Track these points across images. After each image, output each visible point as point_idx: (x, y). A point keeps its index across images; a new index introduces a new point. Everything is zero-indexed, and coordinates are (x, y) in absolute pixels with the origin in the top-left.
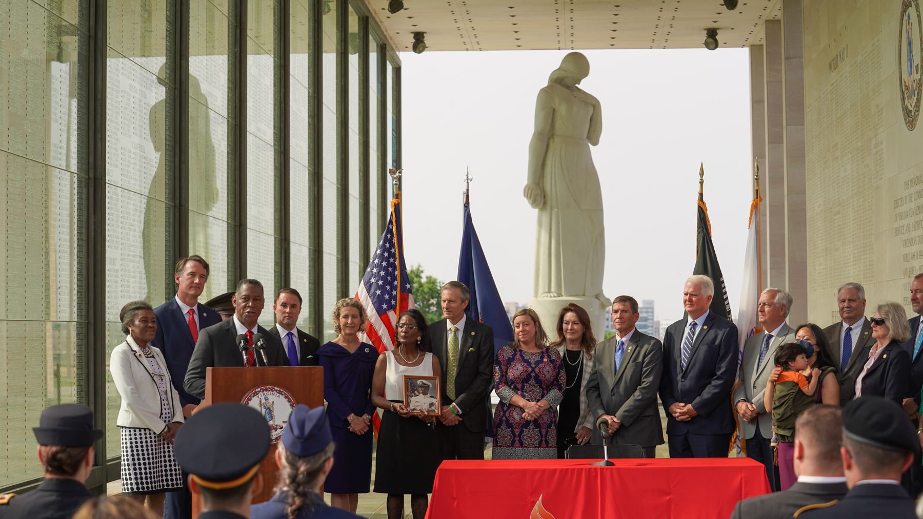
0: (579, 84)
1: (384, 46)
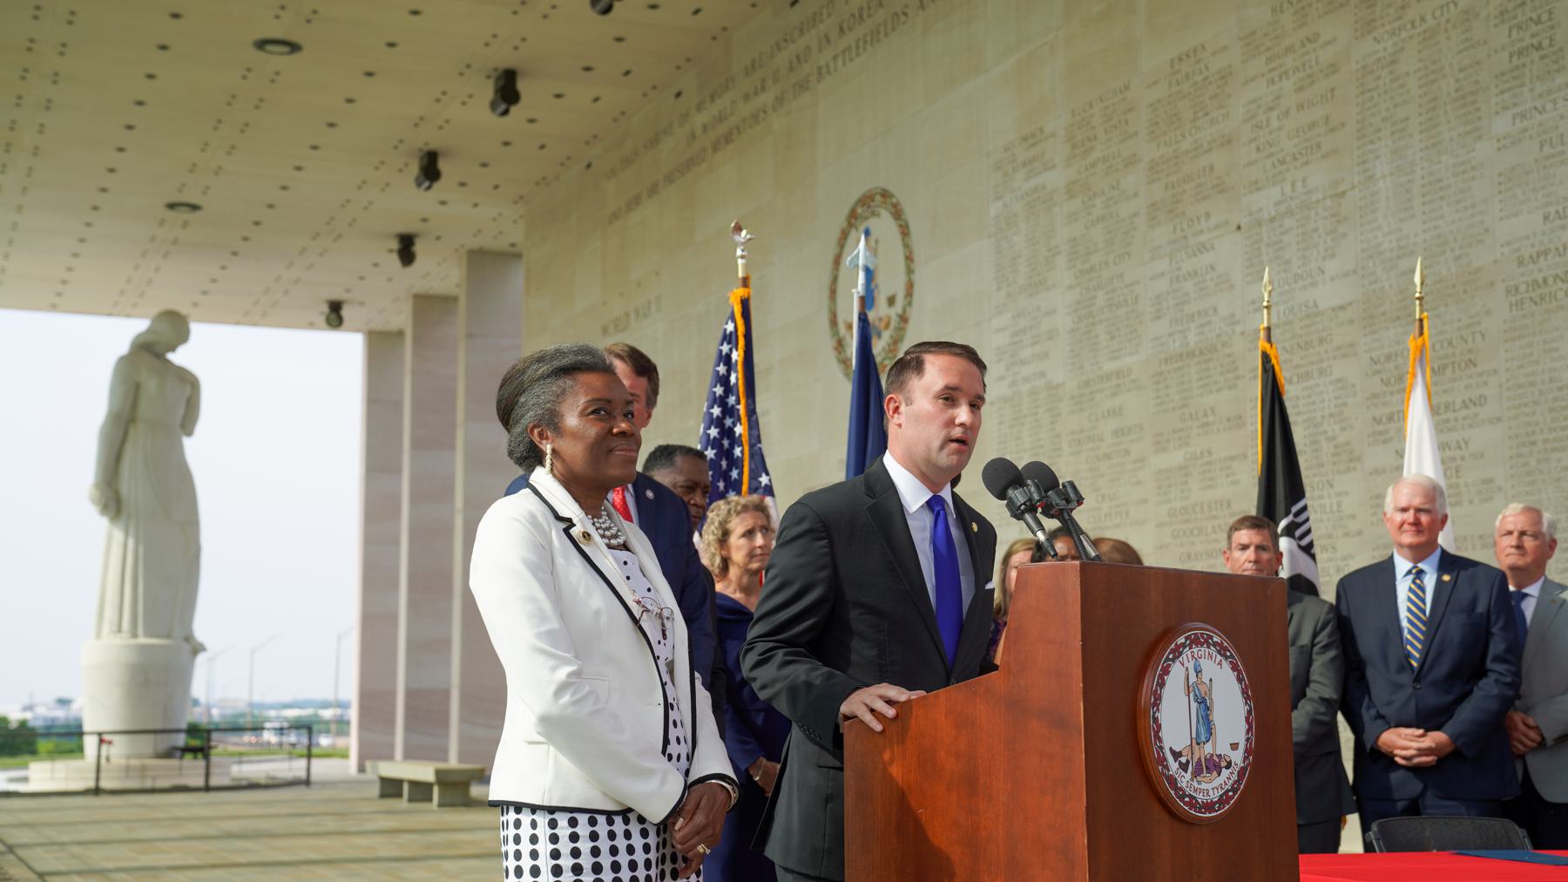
0: (173, 349)
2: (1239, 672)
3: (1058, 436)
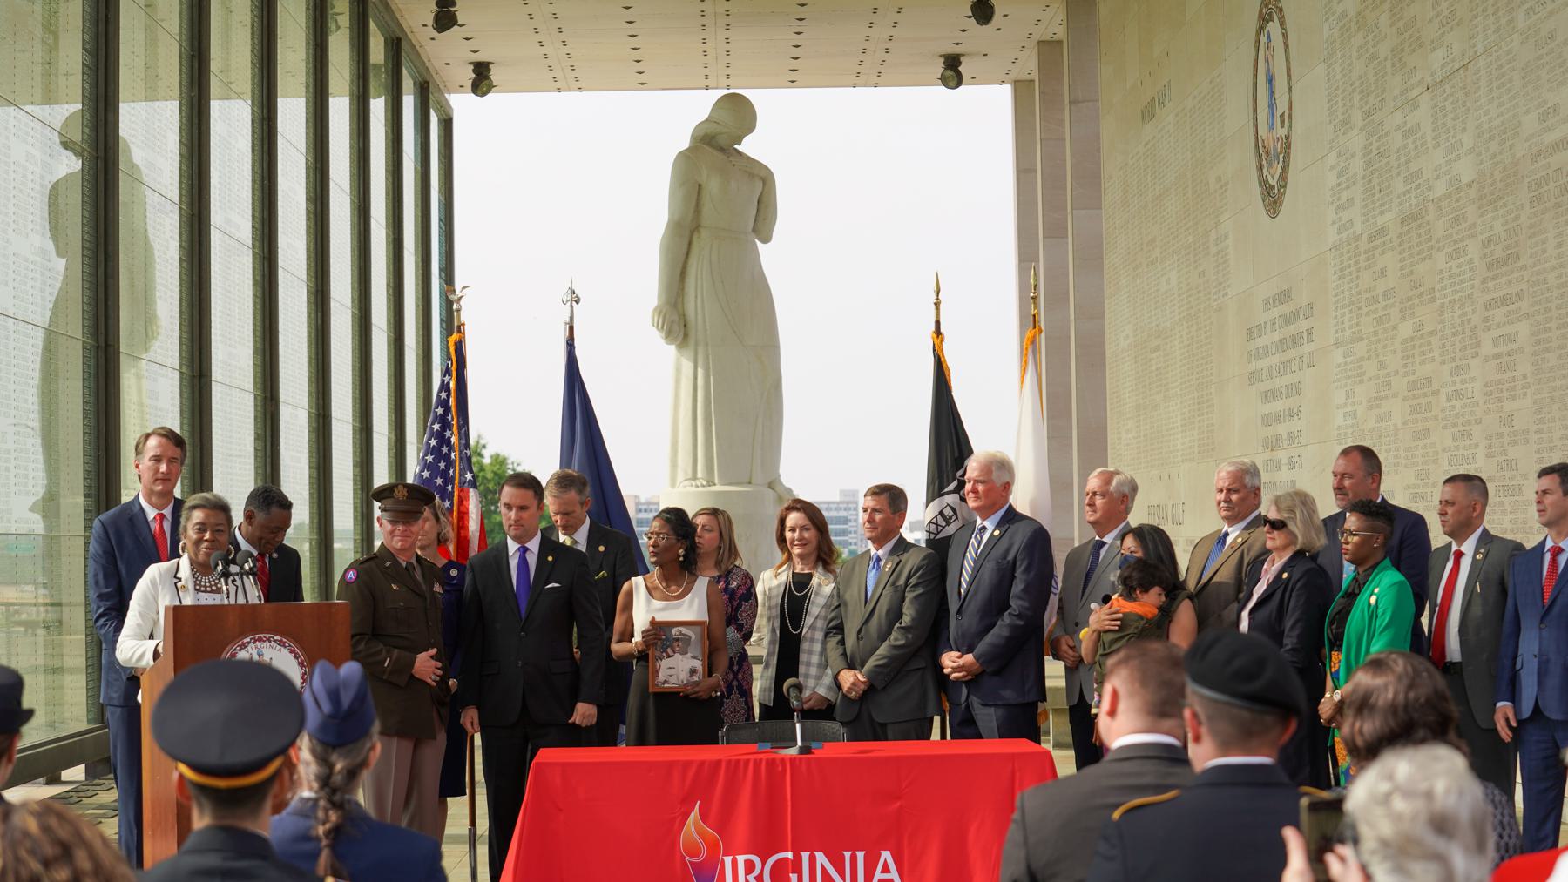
1: (426, 85)
2: (296, 654)
3: (1359, 293)
